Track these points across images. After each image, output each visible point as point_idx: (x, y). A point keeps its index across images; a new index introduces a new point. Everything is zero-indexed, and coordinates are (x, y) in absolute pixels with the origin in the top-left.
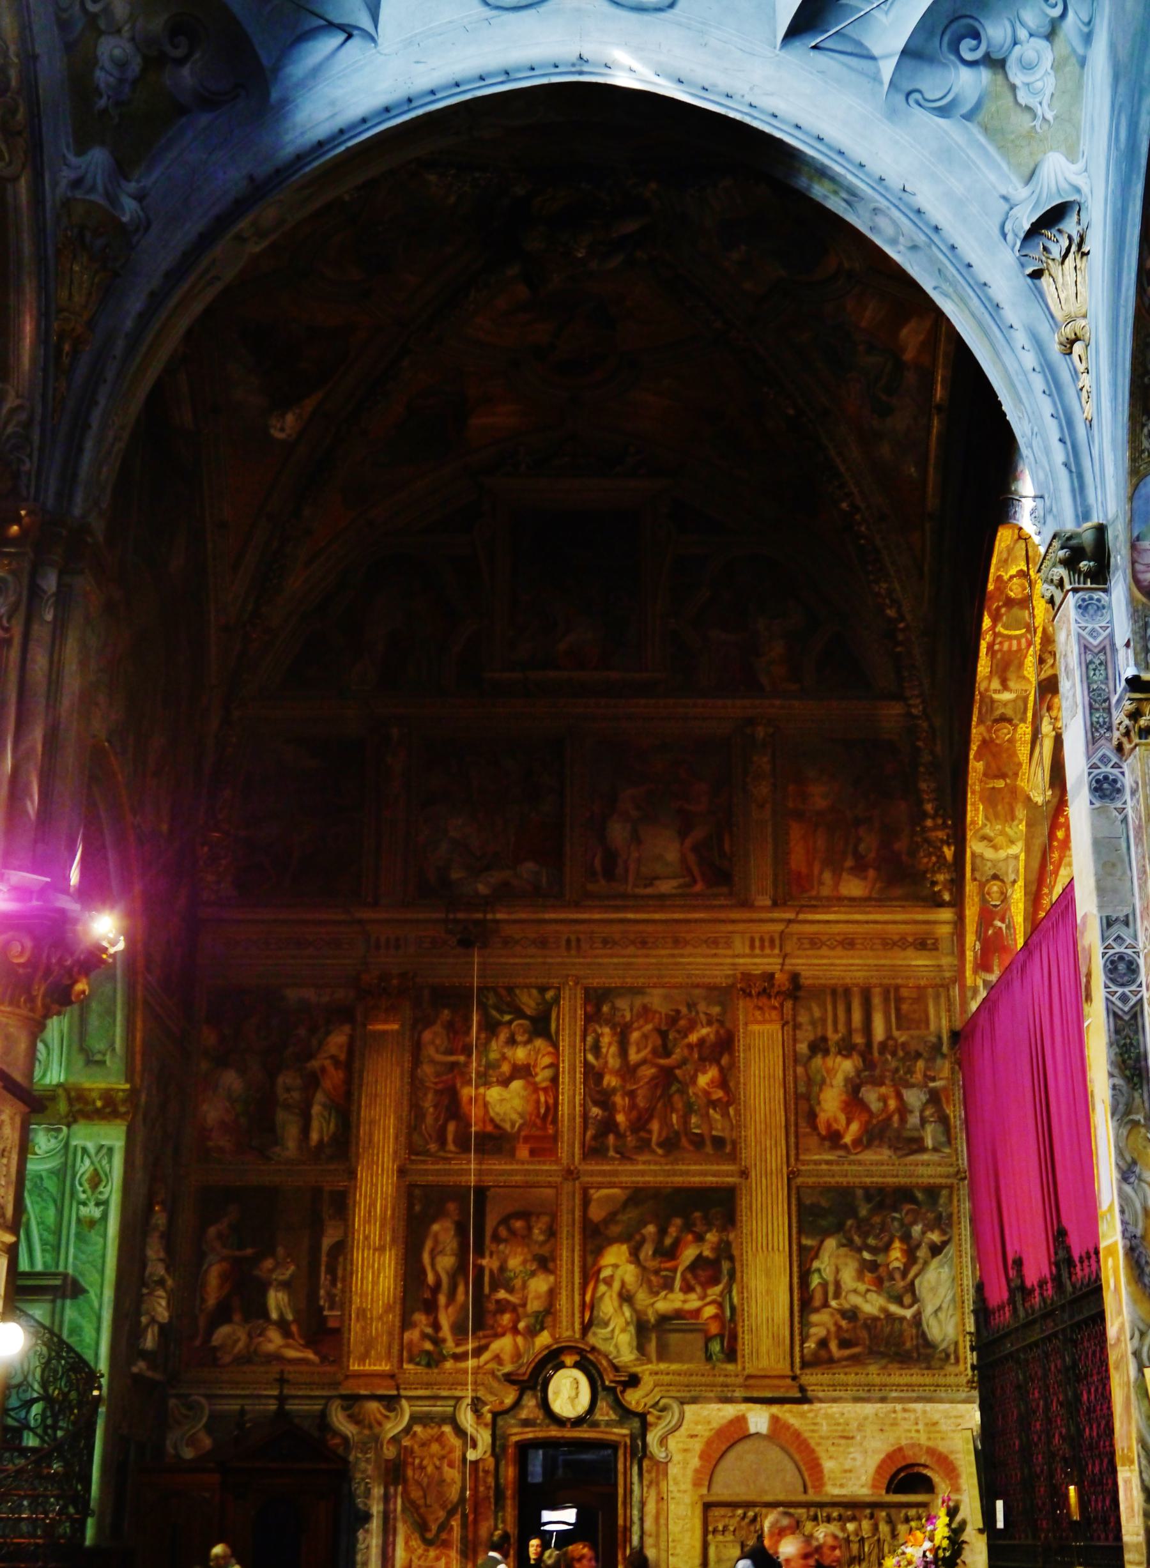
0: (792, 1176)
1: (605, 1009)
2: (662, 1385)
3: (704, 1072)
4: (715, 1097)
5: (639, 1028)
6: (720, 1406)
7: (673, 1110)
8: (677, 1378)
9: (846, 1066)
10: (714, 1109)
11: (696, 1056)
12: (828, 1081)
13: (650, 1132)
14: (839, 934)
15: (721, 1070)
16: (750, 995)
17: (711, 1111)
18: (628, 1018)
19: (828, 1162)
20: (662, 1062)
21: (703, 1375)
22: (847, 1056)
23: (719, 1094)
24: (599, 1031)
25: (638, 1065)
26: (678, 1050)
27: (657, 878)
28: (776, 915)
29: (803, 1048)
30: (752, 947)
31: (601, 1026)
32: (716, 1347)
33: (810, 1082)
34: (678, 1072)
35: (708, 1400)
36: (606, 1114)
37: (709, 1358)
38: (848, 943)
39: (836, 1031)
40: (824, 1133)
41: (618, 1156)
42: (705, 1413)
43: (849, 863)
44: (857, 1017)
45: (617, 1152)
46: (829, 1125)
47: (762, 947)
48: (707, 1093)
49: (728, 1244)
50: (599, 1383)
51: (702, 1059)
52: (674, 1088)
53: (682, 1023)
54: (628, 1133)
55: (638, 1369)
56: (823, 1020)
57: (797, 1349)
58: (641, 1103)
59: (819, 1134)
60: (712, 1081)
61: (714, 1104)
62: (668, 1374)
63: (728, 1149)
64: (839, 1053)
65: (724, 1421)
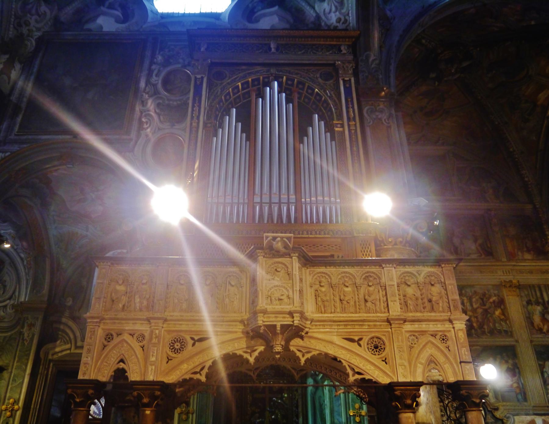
0: (531, 341)
1: (463, 292)
2: (506, 410)
3: (497, 311)
4: (502, 318)
5: (474, 298)
6: (525, 416)
7: (490, 322)
8: (511, 407)
9: (539, 308)
10: (502, 322)
11: (493, 306)
12: (534, 313)
13: (484, 329)
14: (528, 269)
15: (502, 310)
16: (506, 287)
17: (502, 322)
18: (471, 294)
19: (541, 338)
20: (484, 307)
21: (511, 406)
22: (538, 305)
23: (502, 317)
24: (463, 298)
25: (477, 309)
26: (487, 304)
27: (470, 254)
28: (510, 264)
29: (525, 303)
30: (504, 273)
31: (463, 297)
32: (520, 397)
33: (529, 313)
34: (489, 310)
35: (522, 415)
36: (470, 323)
37: (518, 400)
38: (531, 272)
39: (533, 298)
40: (537, 329)
41: (476, 336)
42: (521, 419)
43: (525, 249)
44: (538, 294)
45: (476, 335)
46: (538, 326)
47: (506, 273)
48: (499, 316)
49: (516, 364)
50: (486, 409)
51: (495, 307)
52: (489, 315)
53: (487, 296)
54: (478, 329)
55: (497, 405)
56: (529, 295)
57: (546, 397)
58: (480, 320)
59: (536, 329)
60: (500, 313)
61: (502, 320)
62: (507, 406)
63: (509, 333)
64: (536, 304)
65: (528, 422)
